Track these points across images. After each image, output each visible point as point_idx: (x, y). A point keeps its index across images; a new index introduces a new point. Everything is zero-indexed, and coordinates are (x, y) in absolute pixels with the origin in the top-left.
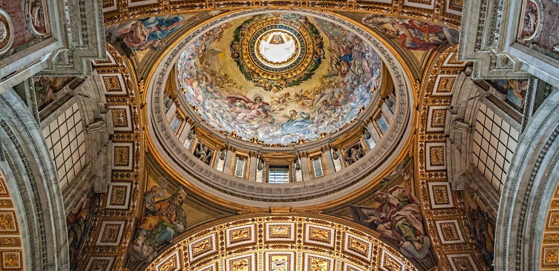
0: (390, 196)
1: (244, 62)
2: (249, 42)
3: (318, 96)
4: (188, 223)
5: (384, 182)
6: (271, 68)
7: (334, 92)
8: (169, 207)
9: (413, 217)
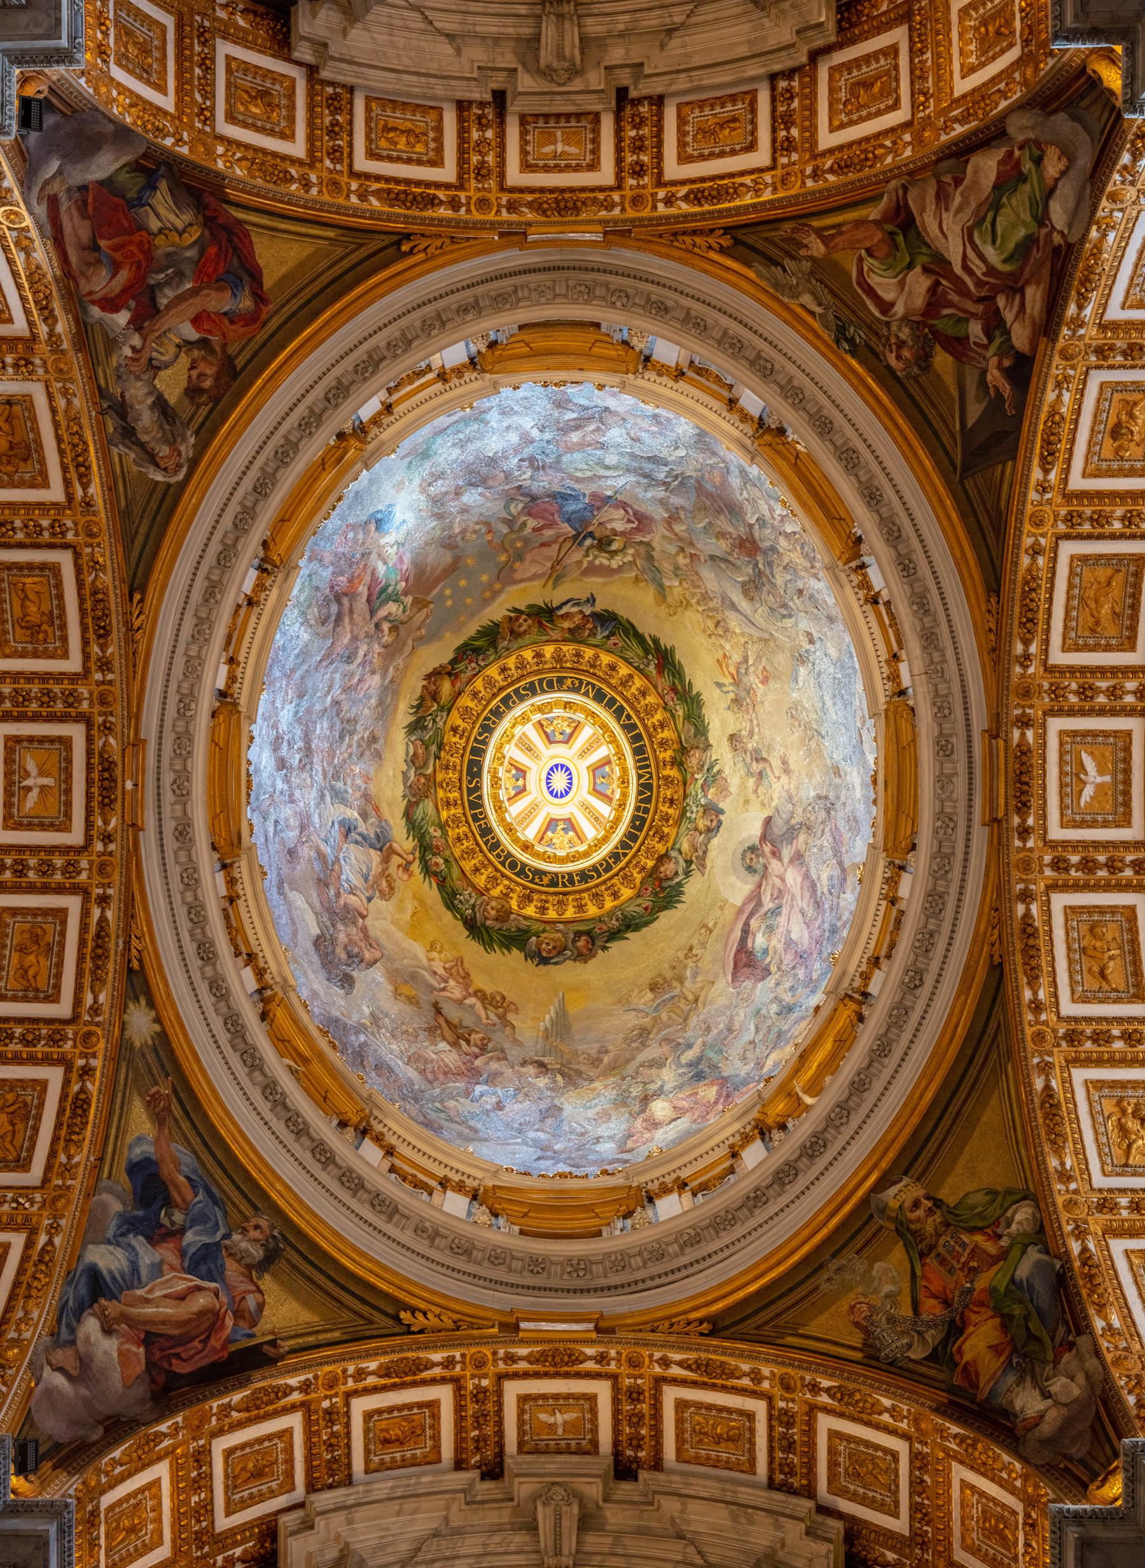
0: (899, 309)
1: (611, 914)
2: (532, 891)
3: (734, 621)
5: (851, 341)
7: (712, 558)
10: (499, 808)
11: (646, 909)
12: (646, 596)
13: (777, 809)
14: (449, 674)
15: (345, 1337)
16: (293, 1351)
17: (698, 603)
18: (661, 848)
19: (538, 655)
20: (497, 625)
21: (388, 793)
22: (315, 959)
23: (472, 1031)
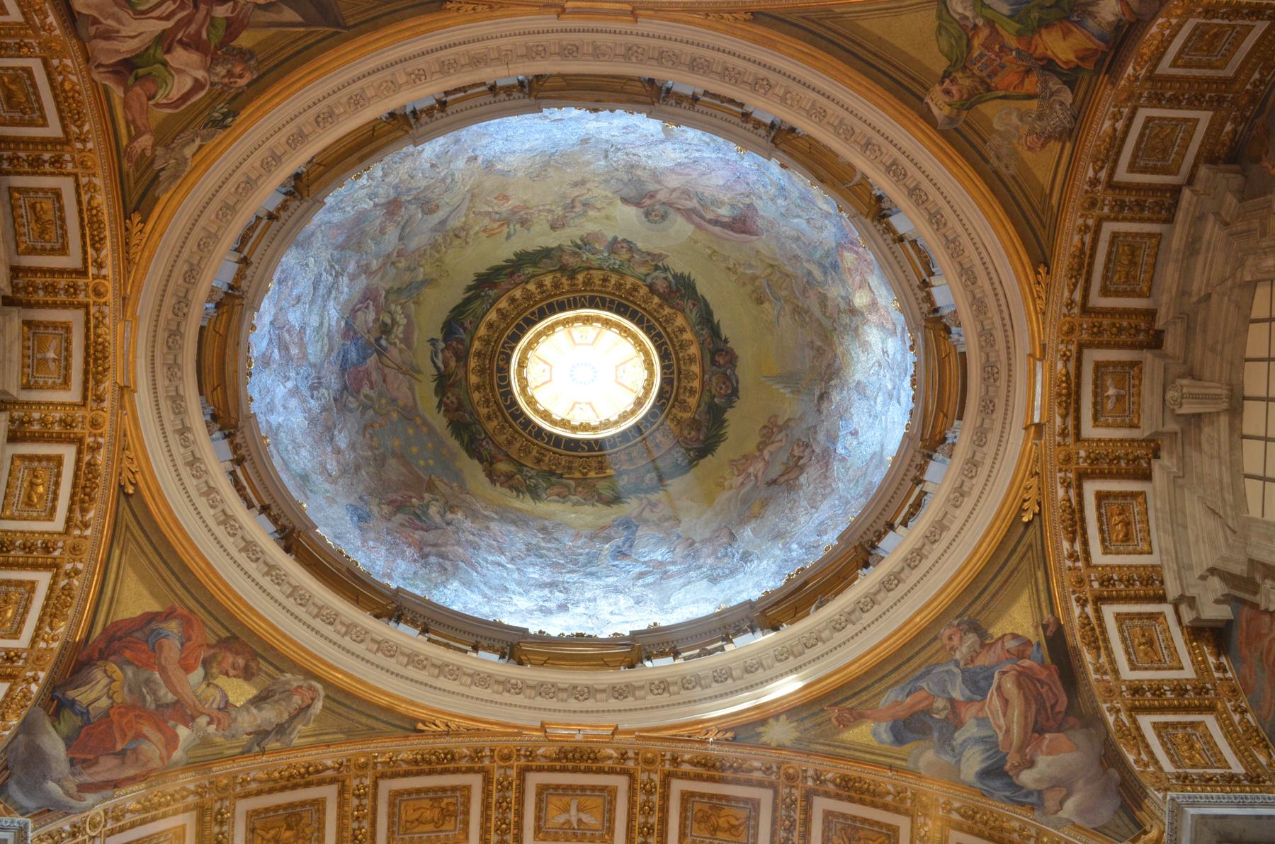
0: (200, 74)
1: (696, 334)
2: (676, 399)
3: (455, 223)
4: (934, 13)
5: (225, 116)
7: (401, 238)
8: (993, 74)
9: (111, 22)
10: (606, 425)
11: (694, 305)
12: (429, 294)
14: (491, 464)
16: (1052, 610)
17: (438, 252)
18: (644, 291)
19: (478, 388)
21: (589, 519)
22: (726, 583)
23: (792, 455)
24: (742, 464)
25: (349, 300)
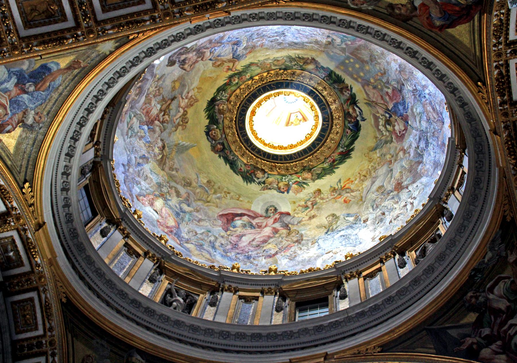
0: (491, 296)
3: (367, 183)
6: (281, 156)
7: (392, 170)
11: (241, 169)
13: (294, 217)
14: (317, 67)
15: (10, 166)
17: (372, 166)
20: (343, 82)
23: (169, 115)
24: (191, 102)
25: (410, 135)
